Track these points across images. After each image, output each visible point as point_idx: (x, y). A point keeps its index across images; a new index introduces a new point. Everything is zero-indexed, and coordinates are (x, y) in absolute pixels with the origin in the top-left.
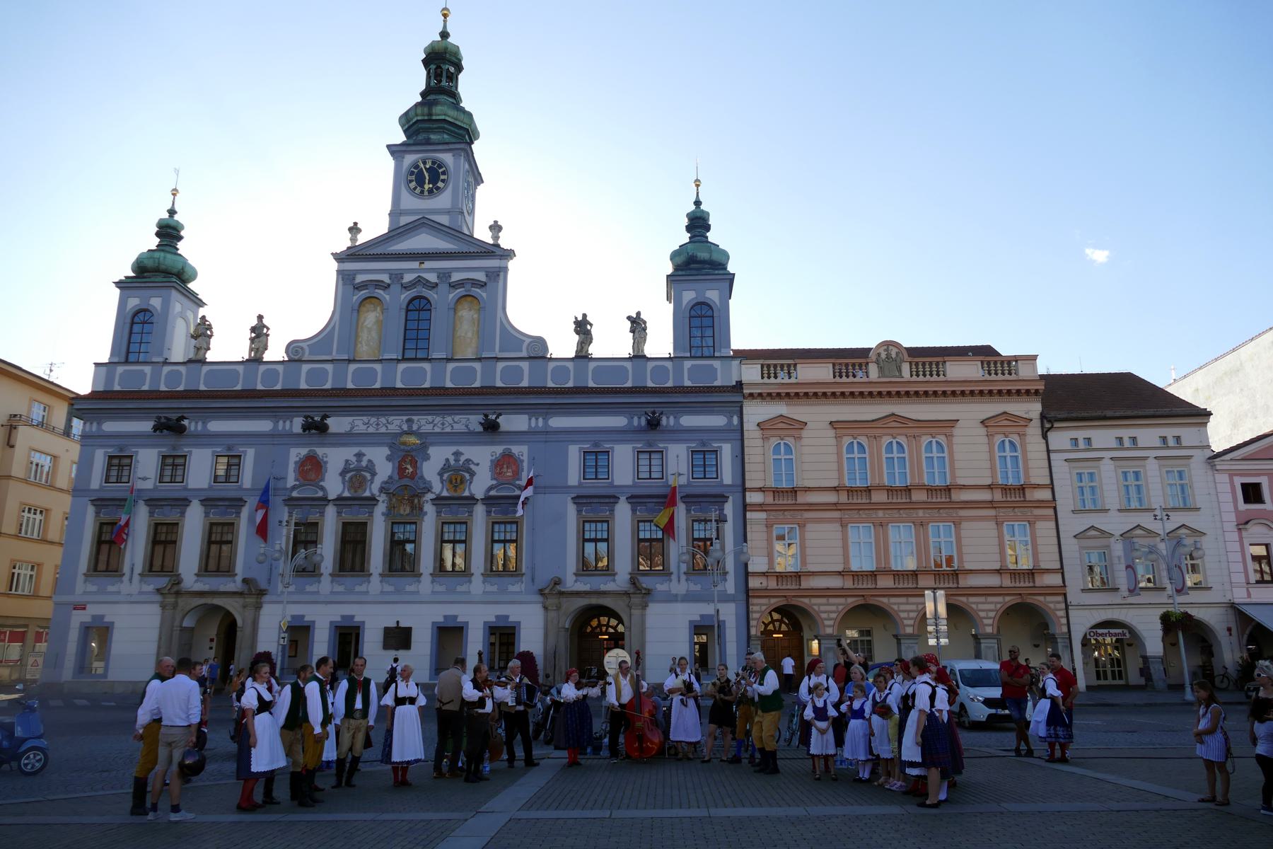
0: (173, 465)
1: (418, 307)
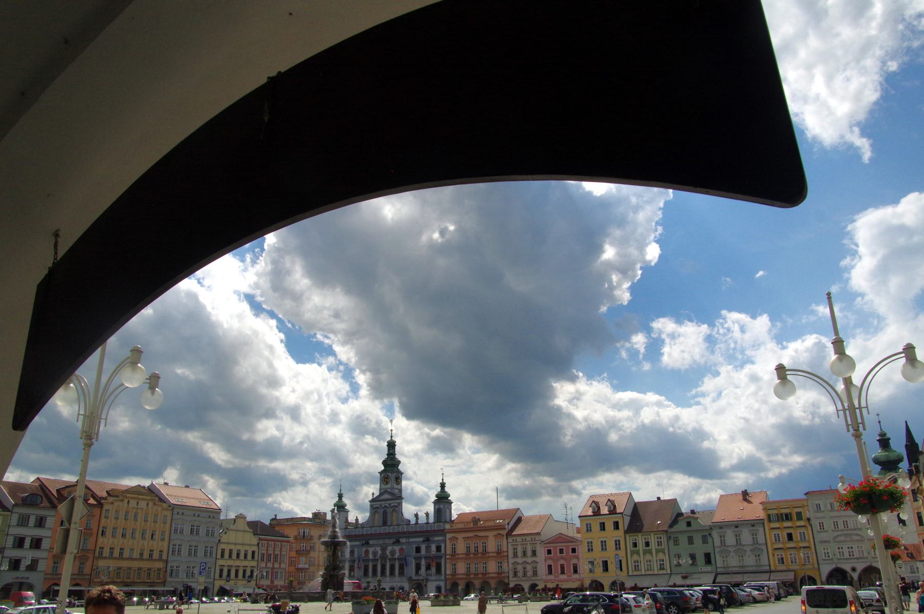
1: (385, 513)
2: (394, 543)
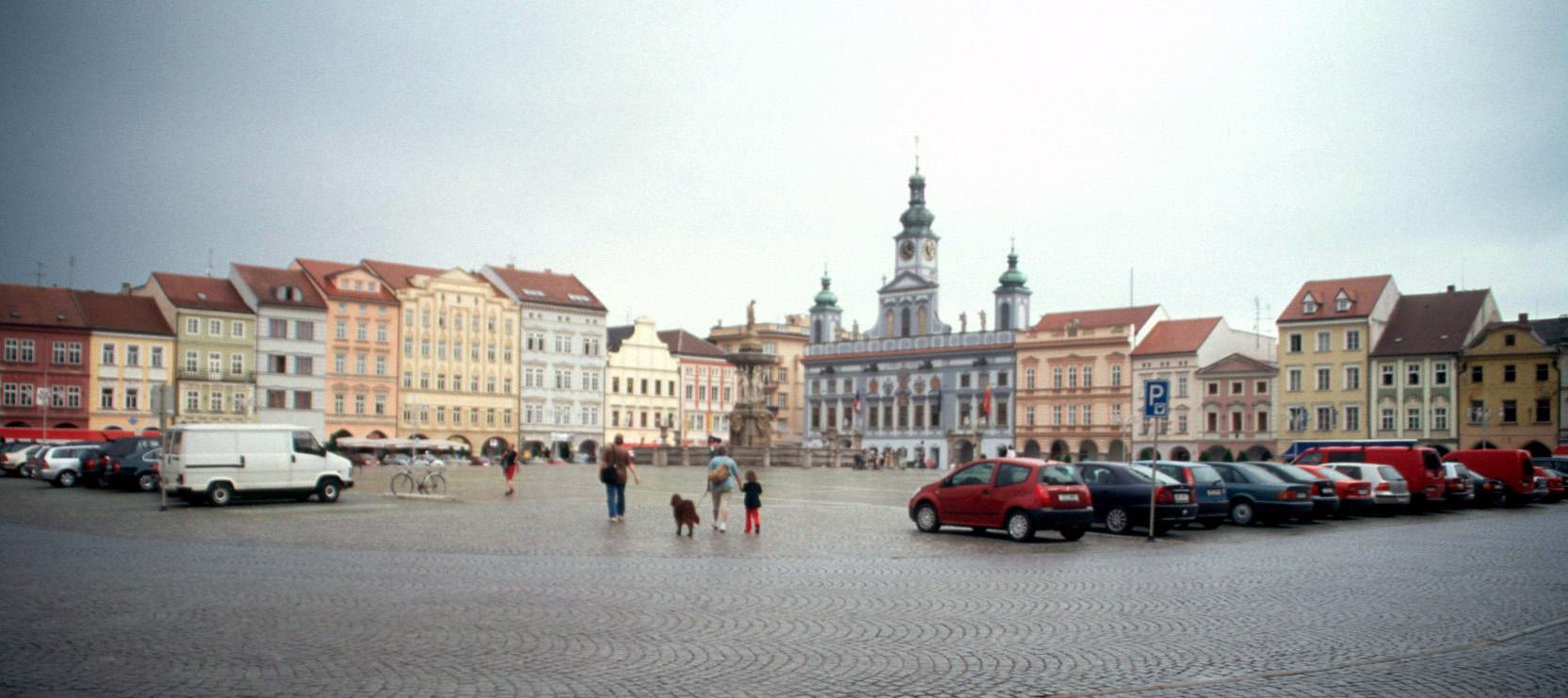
0: (832, 384)
1: (906, 314)
2: (921, 369)
